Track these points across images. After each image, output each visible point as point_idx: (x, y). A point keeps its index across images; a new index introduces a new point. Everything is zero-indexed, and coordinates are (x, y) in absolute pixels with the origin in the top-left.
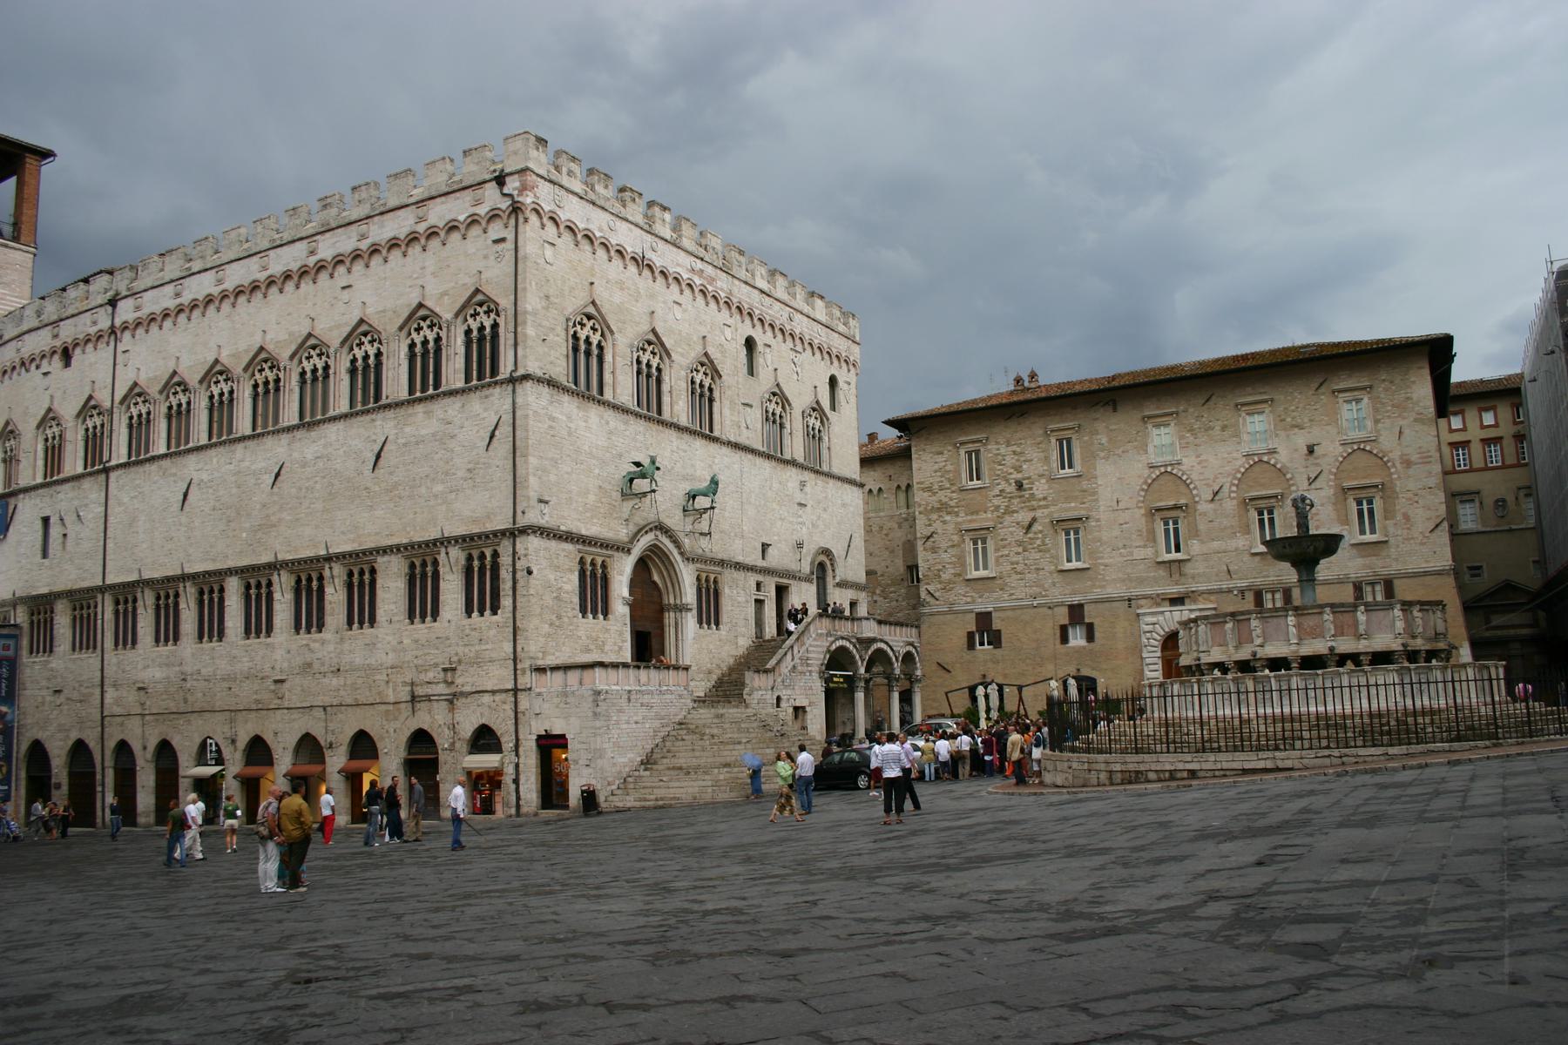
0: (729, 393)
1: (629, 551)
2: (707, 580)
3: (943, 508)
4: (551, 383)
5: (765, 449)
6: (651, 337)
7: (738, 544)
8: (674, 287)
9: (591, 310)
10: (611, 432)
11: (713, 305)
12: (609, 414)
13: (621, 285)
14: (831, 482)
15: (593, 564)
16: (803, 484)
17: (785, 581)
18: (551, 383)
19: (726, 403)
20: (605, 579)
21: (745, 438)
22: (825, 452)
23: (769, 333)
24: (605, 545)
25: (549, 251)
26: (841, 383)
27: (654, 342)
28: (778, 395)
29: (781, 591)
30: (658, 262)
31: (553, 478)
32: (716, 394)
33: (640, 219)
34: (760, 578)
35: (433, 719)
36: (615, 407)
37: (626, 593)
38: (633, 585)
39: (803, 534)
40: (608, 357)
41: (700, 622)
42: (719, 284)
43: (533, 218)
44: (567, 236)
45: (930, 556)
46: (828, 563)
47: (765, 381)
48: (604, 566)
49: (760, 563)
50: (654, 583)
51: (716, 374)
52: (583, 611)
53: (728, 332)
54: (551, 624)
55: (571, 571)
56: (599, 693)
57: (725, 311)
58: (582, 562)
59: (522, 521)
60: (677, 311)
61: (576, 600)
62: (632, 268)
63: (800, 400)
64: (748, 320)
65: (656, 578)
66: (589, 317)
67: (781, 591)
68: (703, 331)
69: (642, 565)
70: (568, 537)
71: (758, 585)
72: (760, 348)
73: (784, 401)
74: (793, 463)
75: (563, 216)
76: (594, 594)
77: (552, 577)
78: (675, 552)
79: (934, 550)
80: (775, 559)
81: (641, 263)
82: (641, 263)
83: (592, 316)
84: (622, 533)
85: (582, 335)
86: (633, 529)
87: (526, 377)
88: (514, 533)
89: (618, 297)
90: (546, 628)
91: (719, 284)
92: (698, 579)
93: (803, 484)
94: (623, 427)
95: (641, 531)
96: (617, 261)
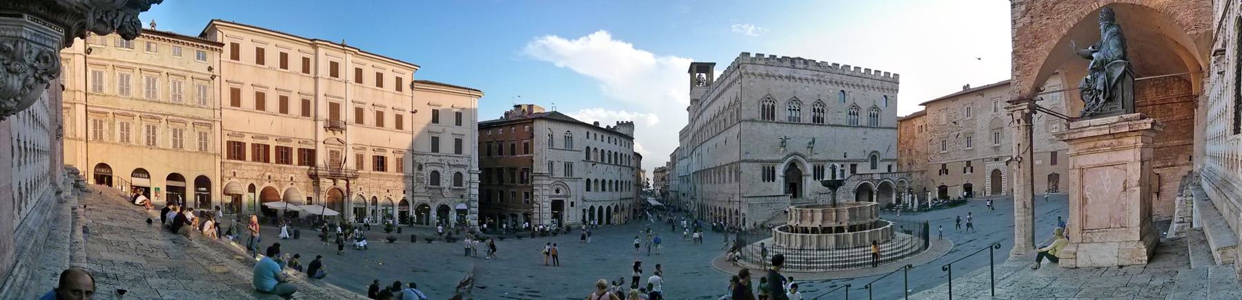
0: (830, 110)
1: (782, 162)
2: (819, 166)
3: (935, 131)
4: (753, 120)
5: (848, 124)
6: (794, 99)
7: (833, 155)
8: (805, 82)
9: (769, 96)
10: (776, 130)
11: (823, 84)
12: (775, 125)
13: (781, 86)
14: (881, 130)
15: (769, 167)
16: (865, 133)
17: (855, 163)
18: (753, 120)
19: (829, 112)
20: (774, 171)
21: (838, 122)
22: (879, 120)
23: (852, 87)
24: (771, 162)
25: (752, 84)
26: (888, 97)
27: (795, 100)
28: (855, 106)
29: (853, 167)
30: (797, 76)
31: (752, 146)
32: (825, 111)
33: (789, 65)
34: (843, 163)
35: (731, 206)
36: (777, 122)
37: (782, 174)
38: (786, 172)
39: (866, 147)
40: (776, 109)
41: (815, 179)
42: (826, 77)
43: (746, 76)
44: (760, 77)
45: (931, 146)
46: (877, 156)
47: (849, 102)
48: (773, 168)
49: (843, 158)
50: (798, 169)
51: (824, 105)
52: (764, 181)
53: (831, 91)
54: (750, 185)
55: (758, 170)
56: (749, 204)
57: (829, 86)
58: (764, 168)
59: (742, 158)
60: (807, 89)
61: (761, 178)
62: (787, 80)
63: (865, 106)
64: (841, 85)
65: (799, 167)
66: (769, 98)
67: (853, 167)
68: (819, 93)
69: (793, 165)
70: (757, 161)
71: (842, 166)
72: (847, 93)
73: (858, 108)
74: (861, 127)
75: (757, 72)
76: (769, 175)
77: (750, 172)
78: (804, 160)
79: (932, 145)
80: (849, 157)
81: (788, 78)
82: (788, 78)
83: (769, 98)
84: (781, 158)
85: (766, 104)
86: (785, 155)
87: (742, 121)
88: (739, 162)
89: (780, 90)
90: (748, 186)
91: (826, 77)
92: (815, 167)
93: (865, 133)
94: (780, 128)
95: (788, 156)
96: (779, 79)
